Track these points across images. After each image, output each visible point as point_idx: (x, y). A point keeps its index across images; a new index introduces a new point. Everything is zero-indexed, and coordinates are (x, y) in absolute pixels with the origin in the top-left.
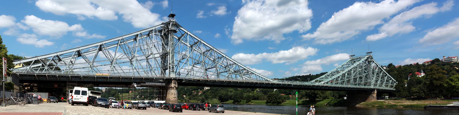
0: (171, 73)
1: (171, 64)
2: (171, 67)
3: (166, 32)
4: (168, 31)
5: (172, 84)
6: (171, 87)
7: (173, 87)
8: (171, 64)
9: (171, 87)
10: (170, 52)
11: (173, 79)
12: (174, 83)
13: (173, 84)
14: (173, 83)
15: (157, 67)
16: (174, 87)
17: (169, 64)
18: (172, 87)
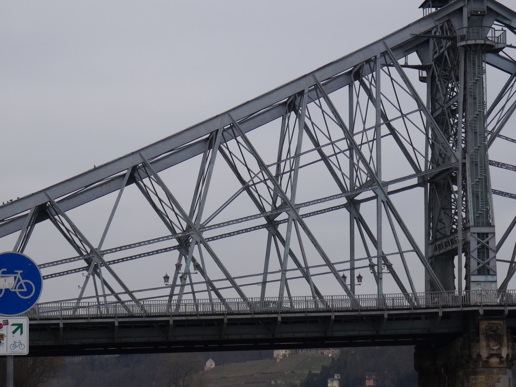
0: (473, 278)
1: (473, 230)
2: (474, 245)
3: (448, 49)
4: (453, 49)
5: (478, 341)
6: (474, 356)
7: (484, 354)
8: (473, 230)
10: (464, 165)
11: (481, 312)
12: (488, 338)
13: (483, 343)
14: (482, 337)
15: (401, 253)
16: (491, 356)
17: (466, 229)
18: (479, 355)
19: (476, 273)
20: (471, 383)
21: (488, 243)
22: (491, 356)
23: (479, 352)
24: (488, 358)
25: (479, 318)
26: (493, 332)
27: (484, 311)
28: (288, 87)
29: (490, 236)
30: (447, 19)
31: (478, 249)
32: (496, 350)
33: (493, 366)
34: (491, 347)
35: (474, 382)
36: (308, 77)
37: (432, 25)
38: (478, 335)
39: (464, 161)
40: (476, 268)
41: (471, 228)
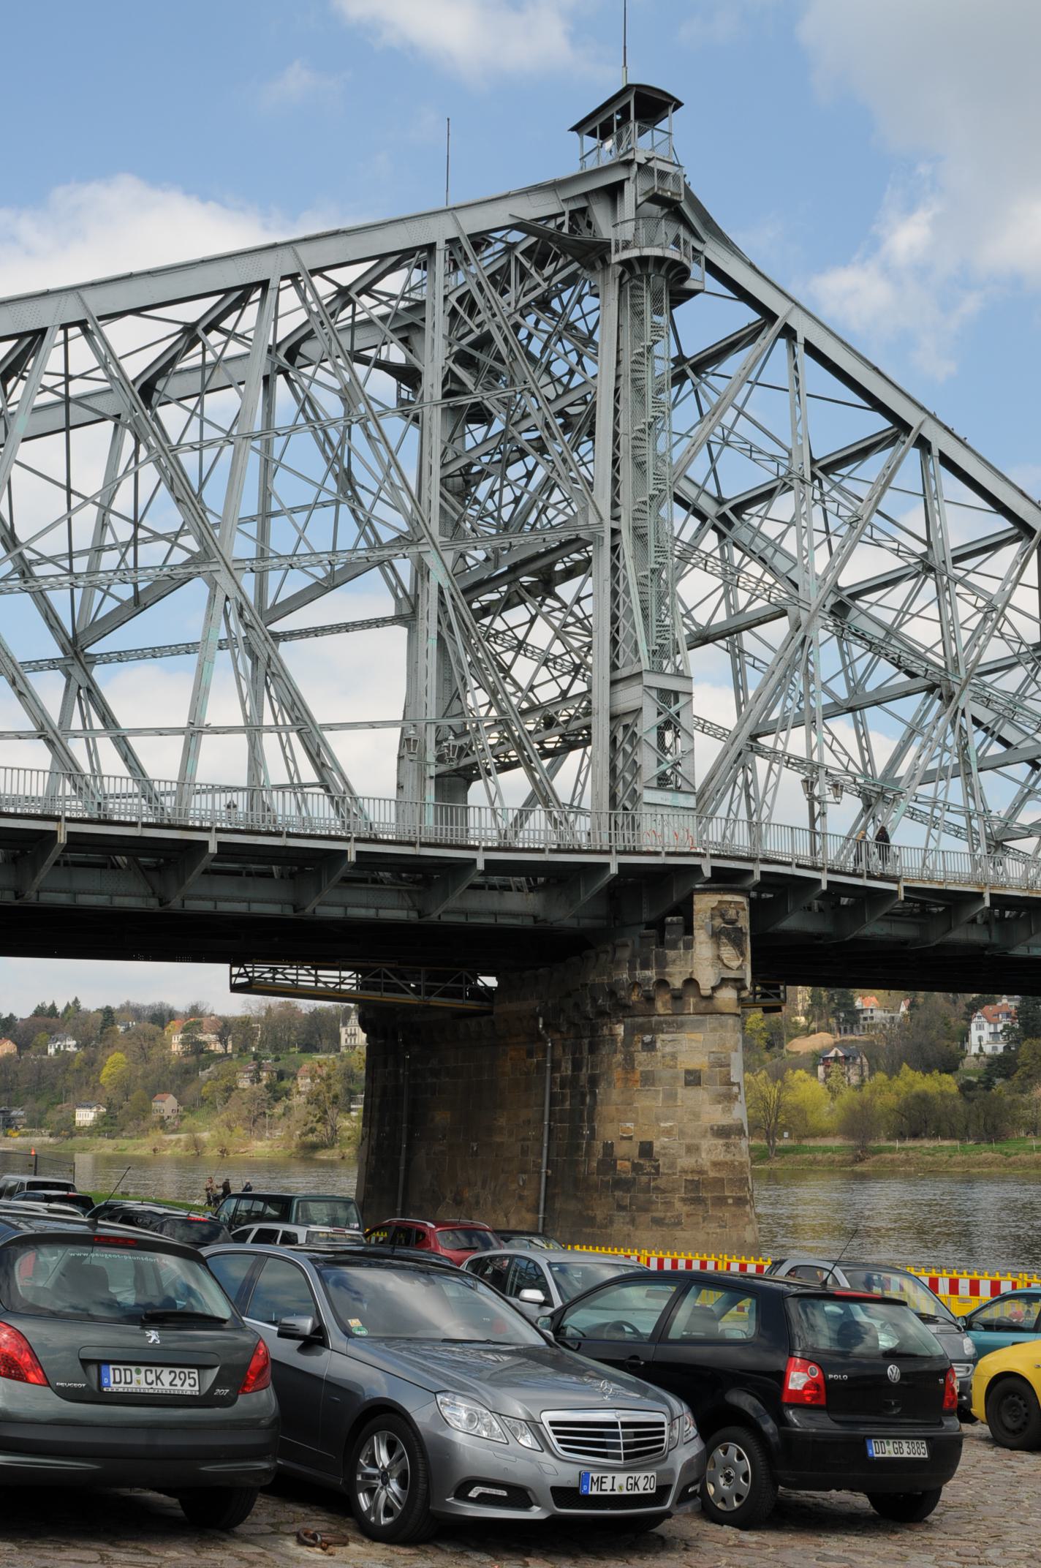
5: (689, 946)
6: (677, 983)
7: (707, 979)
8: (649, 679)
9: (677, 983)
16: (724, 982)
18: (691, 982)
19: (654, 784)
20: (659, 1054)
21: (678, 714)
22: (724, 982)
23: (692, 972)
24: (714, 989)
25: (698, 886)
26: (727, 923)
27: (714, 869)
28: (230, 263)
29: (683, 699)
30: (581, 204)
31: (659, 728)
32: (738, 969)
33: (727, 1011)
34: (725, 961)
35: (668, 1049)
36: (280, 252)
37: (554, 209)
38: (689, 929)
39: (615, 525)
40: (656, 772)
41: (644, 675)
